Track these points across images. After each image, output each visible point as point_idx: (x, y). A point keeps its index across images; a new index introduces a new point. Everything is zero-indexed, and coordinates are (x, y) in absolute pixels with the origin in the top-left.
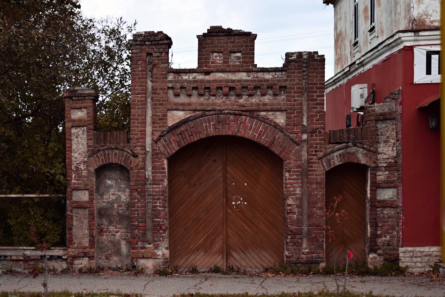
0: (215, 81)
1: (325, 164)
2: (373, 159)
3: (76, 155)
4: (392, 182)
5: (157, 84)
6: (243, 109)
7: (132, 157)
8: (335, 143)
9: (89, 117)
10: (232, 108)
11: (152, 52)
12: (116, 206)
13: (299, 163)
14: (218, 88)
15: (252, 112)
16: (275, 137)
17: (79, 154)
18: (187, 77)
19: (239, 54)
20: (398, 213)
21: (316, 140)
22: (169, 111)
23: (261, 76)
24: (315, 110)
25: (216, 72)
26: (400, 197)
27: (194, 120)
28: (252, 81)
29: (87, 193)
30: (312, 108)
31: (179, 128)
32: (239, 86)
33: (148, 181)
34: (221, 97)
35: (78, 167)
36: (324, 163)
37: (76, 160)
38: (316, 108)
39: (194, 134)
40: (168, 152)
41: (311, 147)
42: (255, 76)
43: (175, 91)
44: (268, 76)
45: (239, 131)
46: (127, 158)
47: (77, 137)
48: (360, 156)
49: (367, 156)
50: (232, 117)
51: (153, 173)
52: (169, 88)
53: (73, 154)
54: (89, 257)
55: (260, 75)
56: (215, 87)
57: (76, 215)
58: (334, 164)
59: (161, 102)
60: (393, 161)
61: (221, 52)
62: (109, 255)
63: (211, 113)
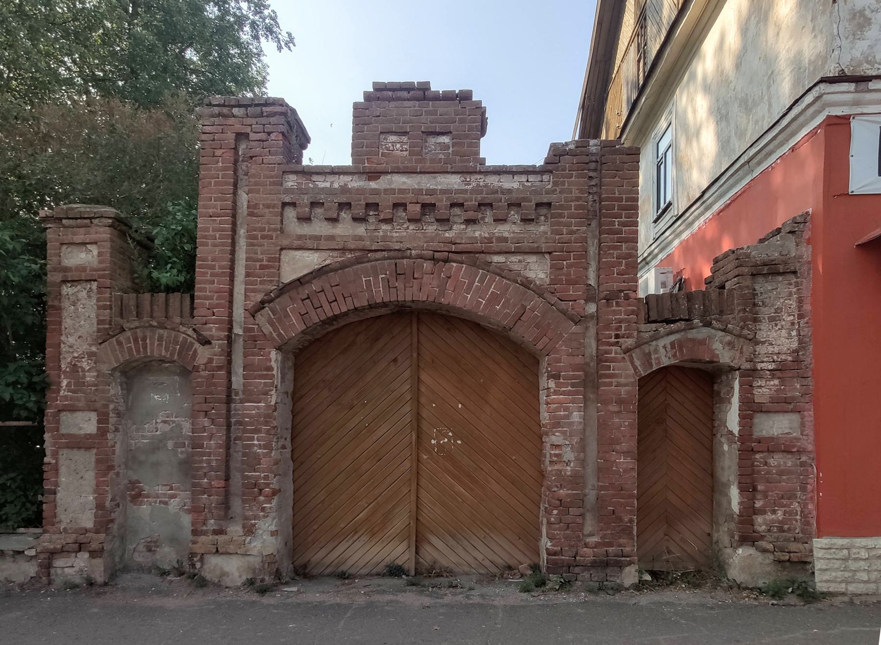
0: (392, 191)
1: (637, 363)
2: (746, 355)
3: (71, 340)
4: (787, 401)
6: (453, 248)
7: (197, 345)
8: (660, 322)
9: (100, 262)
10: (428, 246)
11: (248, 130)
12: (170, 444)
13: (579, 360)
14: (396, 205)
15: (474, 256)
16: (524, 307)
17: (79, 337)
18: (328, 185)
19: (445, 139)
20: (803, 464)
22: (284, 252)
23: (496, 183)
24: (616, 253)
25: (392, 172)
26: (810, 431)
27: (341, 269)
28: (473, 191)
29: (94, 416)
30: (610, 248)
32: (443, 202)
33: (237, 394)
34: (405, 226)
35: (75, 365)
38: (619, 248)
39: (340, 299)
40: (279, 335)
41: (607, 327)
42: (481, 184)
43: (299, 210)
44: (508, 183)
45: (442, 293)
46: (186, 347)
47: (74, 304)
48: (717, 346)
49: (733, 347)
50: (427, 265)
51: (245, 377)
52: (284, 204)
53: (63, 338)
54: (90, 552)
55: (493, 181)
58: (659, 363)
59: (265, 233)
60: (790, 358)
61: (405, 133)
63: (379, 255)
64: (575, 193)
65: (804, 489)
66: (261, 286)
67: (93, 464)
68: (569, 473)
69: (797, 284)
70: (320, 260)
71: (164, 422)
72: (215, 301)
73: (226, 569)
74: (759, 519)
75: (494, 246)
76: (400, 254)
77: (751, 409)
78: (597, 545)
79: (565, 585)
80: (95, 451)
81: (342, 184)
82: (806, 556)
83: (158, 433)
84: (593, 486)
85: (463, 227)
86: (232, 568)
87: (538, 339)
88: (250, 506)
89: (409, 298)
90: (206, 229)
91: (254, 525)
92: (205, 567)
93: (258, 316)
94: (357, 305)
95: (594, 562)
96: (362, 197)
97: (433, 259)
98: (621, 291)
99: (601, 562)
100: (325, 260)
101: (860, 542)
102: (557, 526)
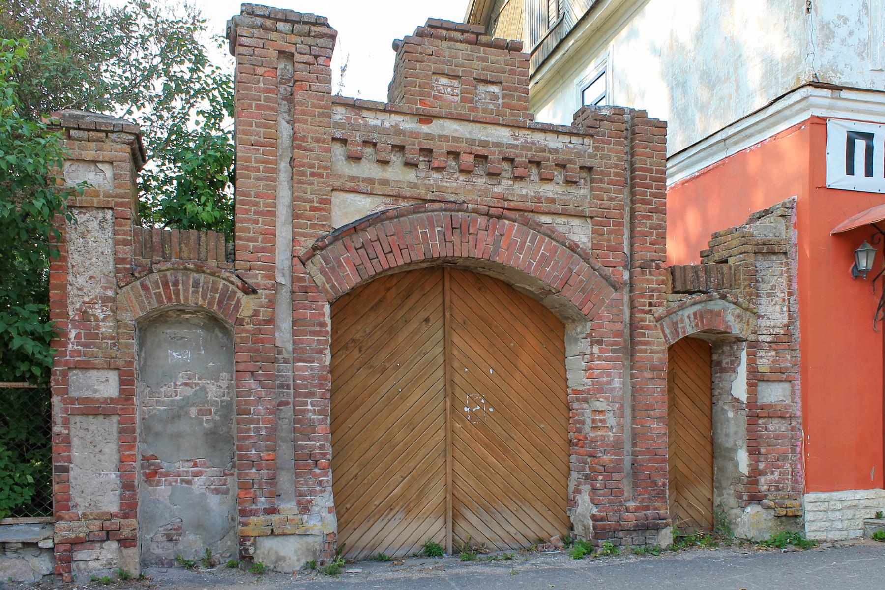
0: (444, 138)
1: (667, 331)
2: (752, 327)
5: (305, 126)
12: (193, 412)
15: (524, 214)
16: (571, 271)
20: (793, 429)
21: (651, 281)
22: (334, 193)
23: (542, 141)
26: (798, 399)
27: (397, 217)
28: (523, 148)
29: (113, 377)
30: (644, 217)
31: (361, 233)
32: (495, 156)
36: (666, 328)
37: (80, 293)
38: (650, 218)
39: (396, 250)
41: (642, 296)
42: (529, 140)
46: (226, 297)
48: (730, 318)
49: (742, 319)
50: (482, 221)
55: (539, 138)
56: (445, 151)
57: (82, 433)
58: (684, 333)
59: (315, 170)
60: (782, 332)
62: (176, 530)
63: (436, 206)
64: (614, 160)
65: (793, 451)
66: (312, 231)
67: (115, 435)
68: (611, 439)
69: (787, 264)
70: (373, 206)
71: (186, 384)
72: (260, 244)
73: (282, 553)
74: (762, 480)
75: (545, 206)
76: (456, 207)
77: (755, 378)
78: (637, 509)
79: (612, 551)
80: (115, 419)
81: (393, 124)
82: (798, 510)
83: (178, 398)
84: (628, 452)
85: (511, 182)
86: (290, 551)
87: (583, 304)
88: (306, 481)
89: (465, 255)
90: (248, 160)
91: (310, 502)
92: (258, 552)
93: (309, 262)
94: (414, 258)
95: (637, 525)
96: (417, 141)
97: (487, 215)
98: (653, 260)
99: (643, 525)
100: (377, 207)
101: (837, 495)
102: (602, 492)
